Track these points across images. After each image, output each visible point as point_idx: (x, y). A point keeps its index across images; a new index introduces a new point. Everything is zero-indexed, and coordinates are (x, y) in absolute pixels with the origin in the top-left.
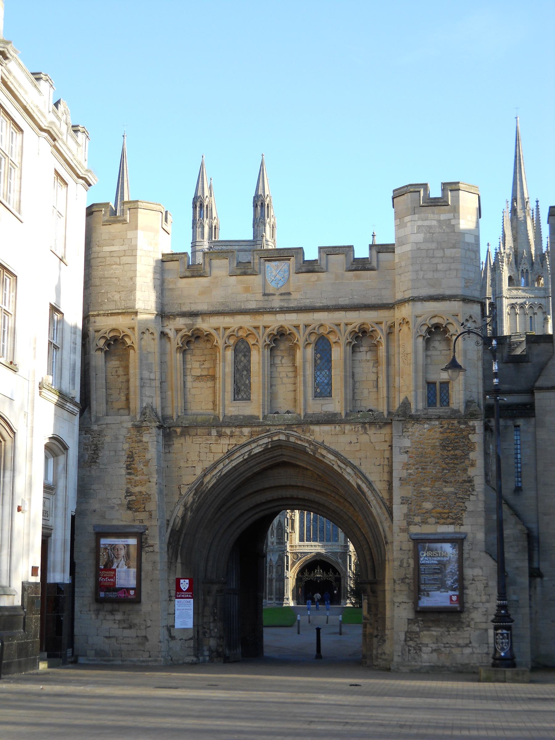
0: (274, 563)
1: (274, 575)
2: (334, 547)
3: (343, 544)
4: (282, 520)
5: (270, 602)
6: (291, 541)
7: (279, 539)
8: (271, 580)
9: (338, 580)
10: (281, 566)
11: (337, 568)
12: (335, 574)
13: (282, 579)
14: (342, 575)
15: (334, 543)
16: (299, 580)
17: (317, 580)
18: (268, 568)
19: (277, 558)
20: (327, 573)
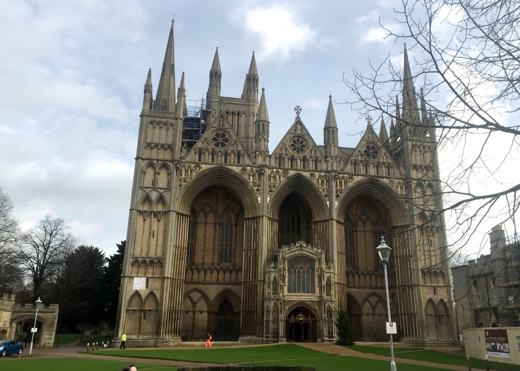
0: (271, 309)
1: (271, 318)
2: (312, 297)
3: (318, 295)
4: (277, 276)
5: (266, 339)
6: (283, 294)
7: (274, 290)
8: (268, 322)
9: (315, 322)
10: (277, 311)
11: (314, 313)
12: (312, 318)
13: (276, 321)
14: (318, 319)
15: (312, 294)
16: (287, 322)
17: (300, 322)
18: (265, 313)
19: (272, 305)
20: (307, 317)
